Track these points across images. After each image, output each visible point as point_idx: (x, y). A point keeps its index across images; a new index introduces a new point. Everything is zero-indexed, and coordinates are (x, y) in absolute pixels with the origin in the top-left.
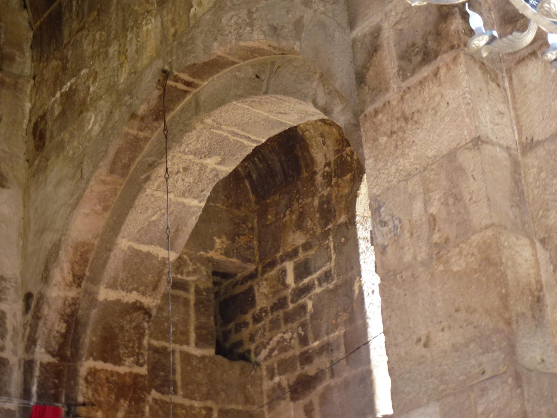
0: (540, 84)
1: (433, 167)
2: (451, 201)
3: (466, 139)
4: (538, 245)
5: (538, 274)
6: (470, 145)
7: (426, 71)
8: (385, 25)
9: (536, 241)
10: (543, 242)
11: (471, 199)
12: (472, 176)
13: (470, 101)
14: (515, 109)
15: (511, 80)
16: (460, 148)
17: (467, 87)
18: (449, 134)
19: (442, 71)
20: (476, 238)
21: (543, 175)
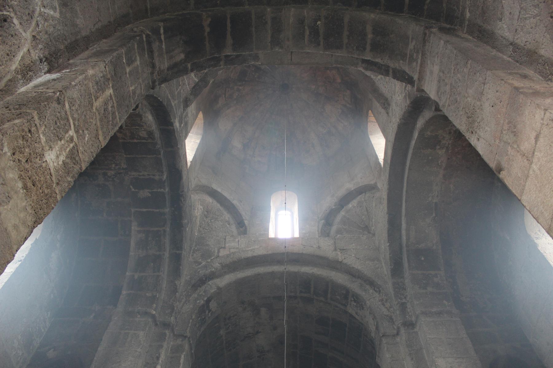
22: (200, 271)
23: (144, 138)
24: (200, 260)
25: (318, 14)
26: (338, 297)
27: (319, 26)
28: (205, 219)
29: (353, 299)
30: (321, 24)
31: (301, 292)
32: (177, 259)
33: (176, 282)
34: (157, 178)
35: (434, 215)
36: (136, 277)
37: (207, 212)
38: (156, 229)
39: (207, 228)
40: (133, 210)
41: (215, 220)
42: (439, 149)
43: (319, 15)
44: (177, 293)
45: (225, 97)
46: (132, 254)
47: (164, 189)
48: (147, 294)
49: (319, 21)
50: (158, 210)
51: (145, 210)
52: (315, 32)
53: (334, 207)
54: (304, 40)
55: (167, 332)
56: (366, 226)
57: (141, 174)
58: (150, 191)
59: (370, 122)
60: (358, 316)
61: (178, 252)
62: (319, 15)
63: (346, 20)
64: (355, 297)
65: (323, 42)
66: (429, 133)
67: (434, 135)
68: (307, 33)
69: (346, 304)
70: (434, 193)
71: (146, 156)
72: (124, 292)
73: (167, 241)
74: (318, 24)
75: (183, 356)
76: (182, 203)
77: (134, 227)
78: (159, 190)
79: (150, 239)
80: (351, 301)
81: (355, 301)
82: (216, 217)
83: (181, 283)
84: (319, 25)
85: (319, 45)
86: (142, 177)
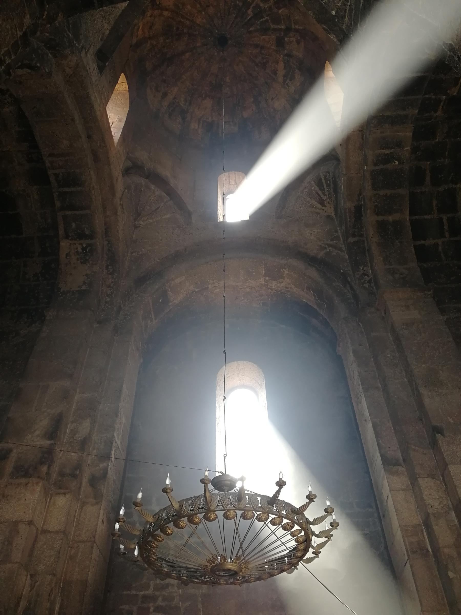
0: (61, 508)
1: (6, 524)
2: (6, 543)
3: (26, 519)
4: (29, 577)
5: (23, 590)
6: (27, 523)
7: (23, 480)
8: (15, 451)
9: (29, 574)
10: (32, 576)
11: (16, 547)
12: (21, 537)
13: (35, 504)
14: (47, 513)
15: (50, 499)
16: (22, 522)
17: (37, 497)
18: (20, 513)
19: (29, 485)
20: (9, 565)
21: (45, 546)
25: (405, 161)
26: (74, 225)
27: (394, 163)
29: (84, 246)
30: (396, 165)
31: (56, 175)
35: (197, 290)
42: (265, 279)
43: (404, 162)
49: (398, 163)
52: (388, 159)
53: (146, 169)
54: (380, 149)
56: (140, 215)
59: (228, 175)
60: (66, 257)
62: (404, 162)
64: (89, 248)
65: (378, 169)
66: (286, 272)
67: (284, 276)
68: (387, 152)
69: (70, 238)
70: (217, 283)
74: (395, 162)
80: (81, 244)
81: (84, 249)
82: (107, 17)
84: (395, 163)
85: (376, 165)
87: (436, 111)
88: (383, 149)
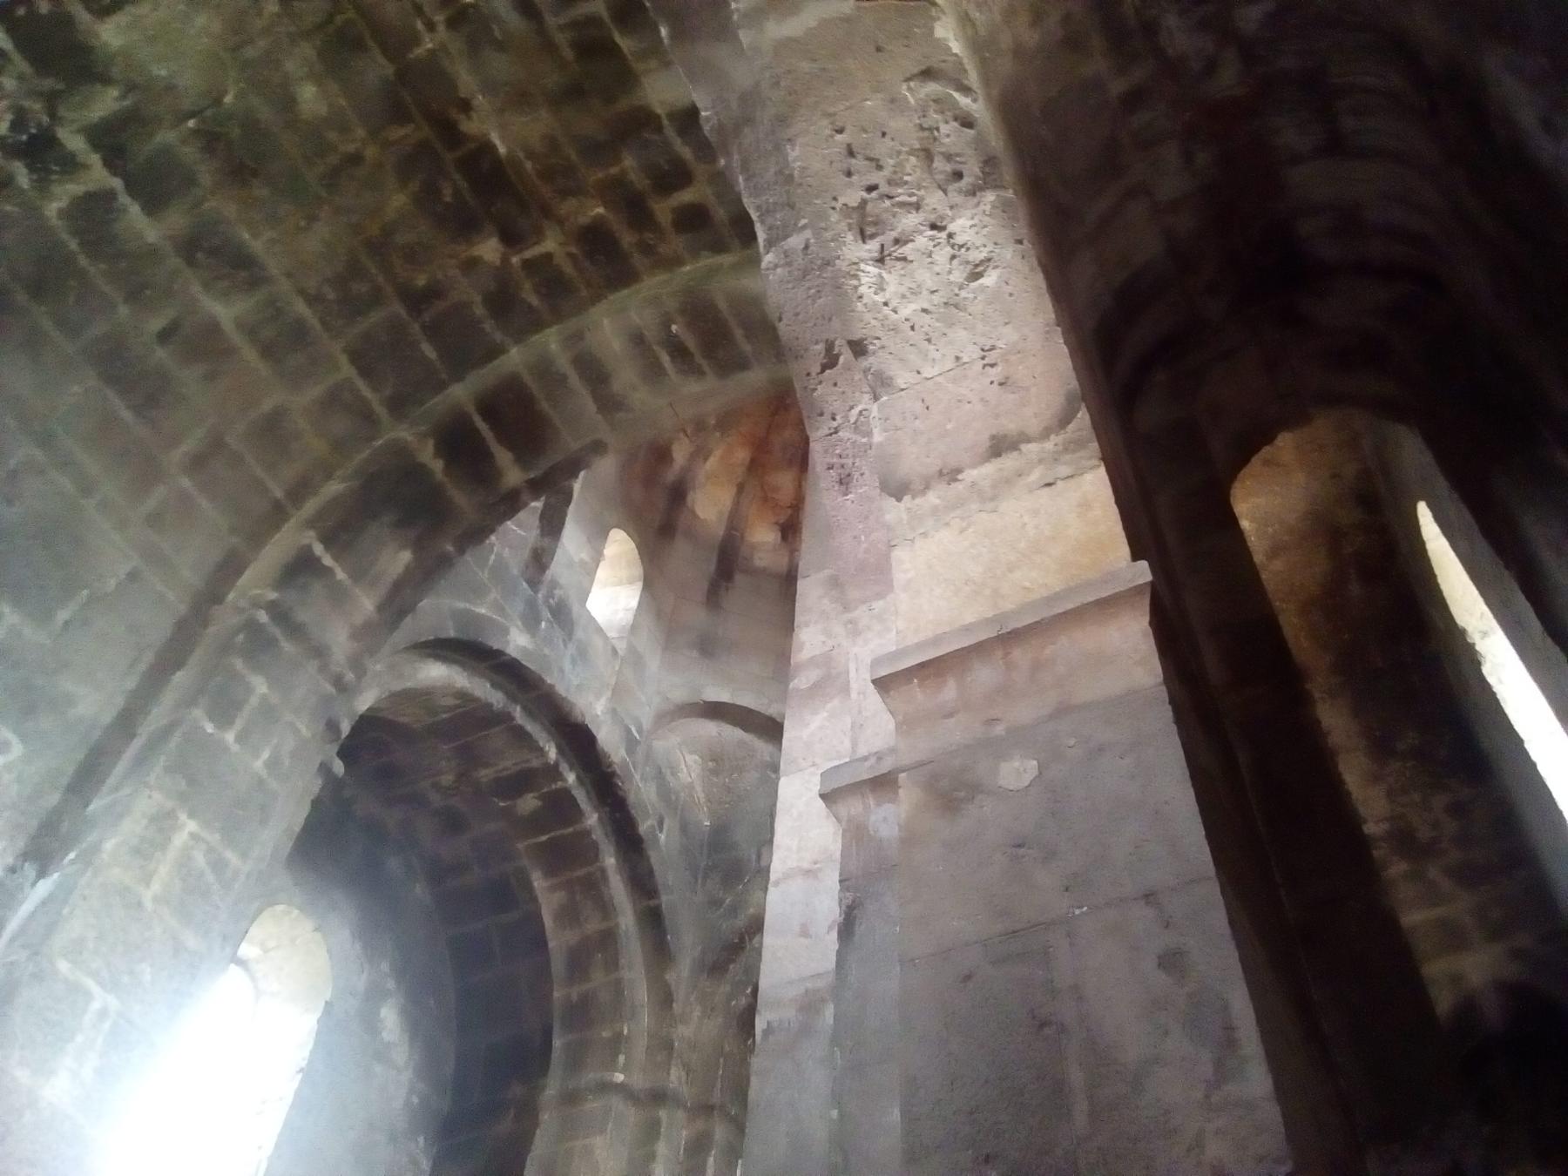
22: (721, 924)
23: (458, 707)
24: (721, 895)
28: (715, 779)
32: (654, 921)
33: (667, 977)
34: (535, 763)
36: (575, 997)
37: (716, 761)
38: (580, 873)
39: (728, 799)
40: (520, 846)
41: (741, 772)
44: (674, 1005)
45: (687, 435)
46: (551, 945)
47: (564, 780)
48: (604, 1034)
50: (571, 830)
51: (544, 838)
52: (679, 351)
54: (668, 375)
55: (663, 1114)
57: (500, 767)
58: (536, 794)
61: (652, 903)
63: (722, 305)
71: (486, 733)
72: (557, 1043)
73: (618, 888)
75: (711, 1160)
76: (621, 790)
77: (539, 882)
78: (554, 787)
79: (578, 897)
83: (681, 974)
86: (505, 773)
87: (548, 257)
88: (664, 369)
